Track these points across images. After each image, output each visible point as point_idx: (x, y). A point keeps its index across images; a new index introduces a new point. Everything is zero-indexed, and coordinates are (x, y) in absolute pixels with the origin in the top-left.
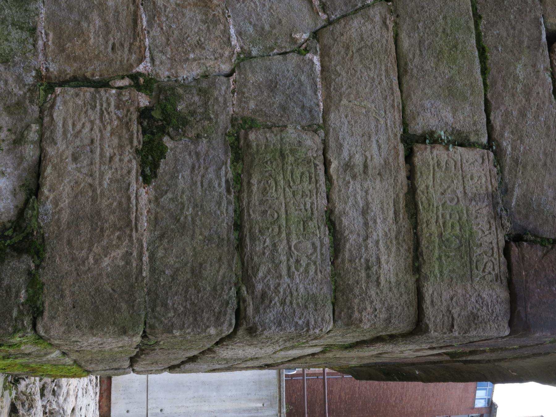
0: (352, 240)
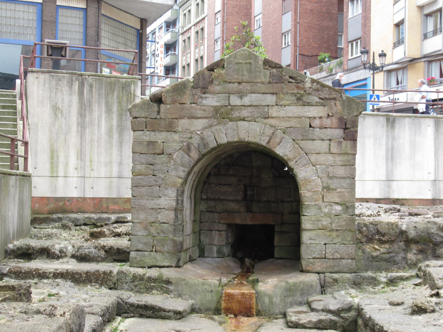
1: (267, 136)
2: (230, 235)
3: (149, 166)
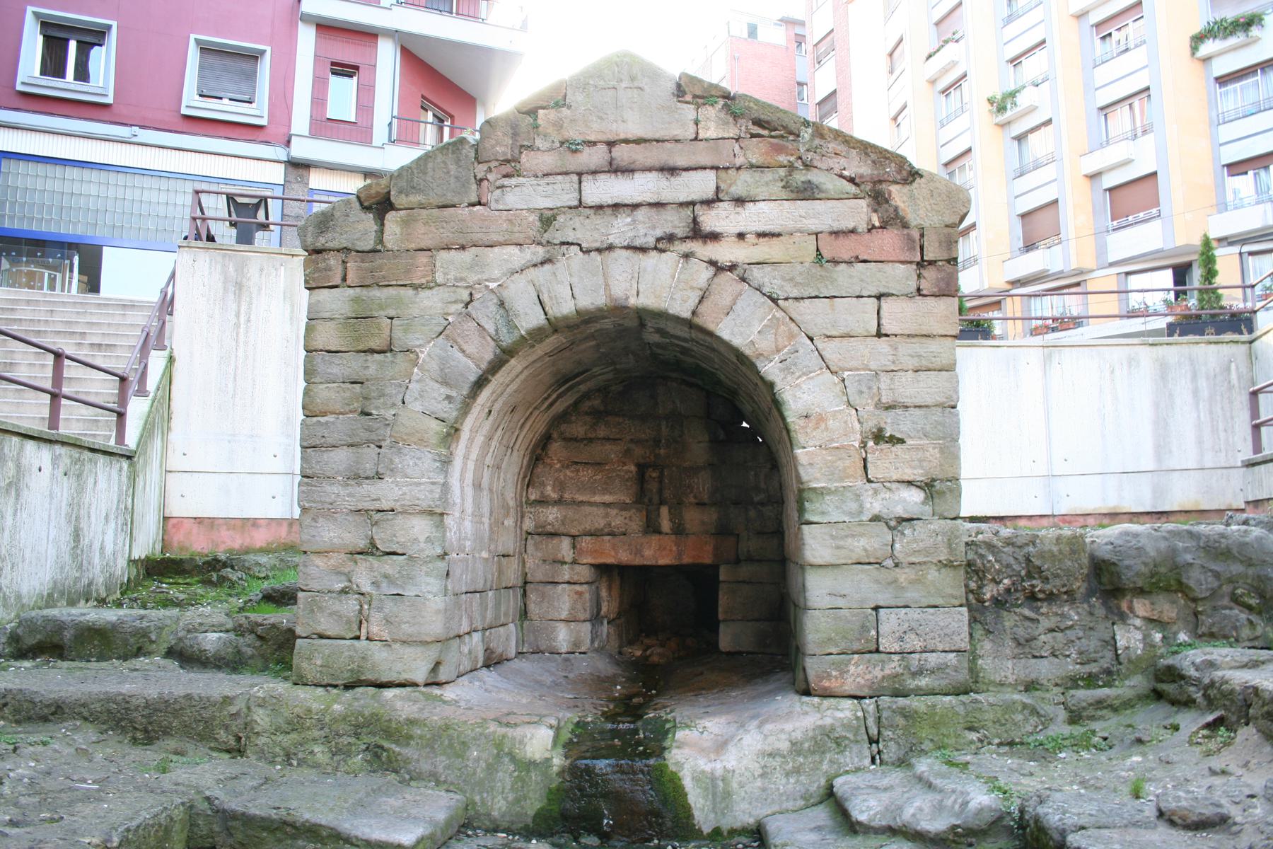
0: (925, 363)
1: (692, 288)
2: (604, 593)
3: (349, 385)
